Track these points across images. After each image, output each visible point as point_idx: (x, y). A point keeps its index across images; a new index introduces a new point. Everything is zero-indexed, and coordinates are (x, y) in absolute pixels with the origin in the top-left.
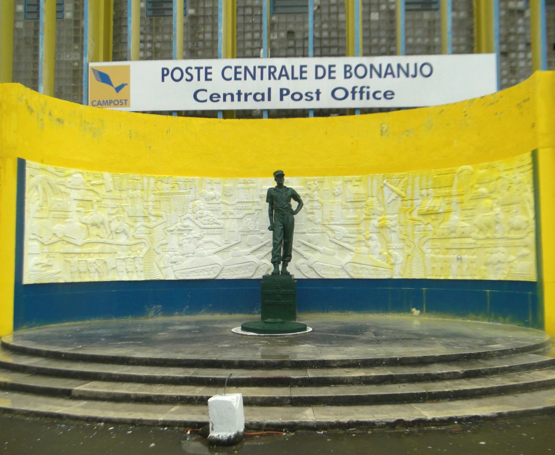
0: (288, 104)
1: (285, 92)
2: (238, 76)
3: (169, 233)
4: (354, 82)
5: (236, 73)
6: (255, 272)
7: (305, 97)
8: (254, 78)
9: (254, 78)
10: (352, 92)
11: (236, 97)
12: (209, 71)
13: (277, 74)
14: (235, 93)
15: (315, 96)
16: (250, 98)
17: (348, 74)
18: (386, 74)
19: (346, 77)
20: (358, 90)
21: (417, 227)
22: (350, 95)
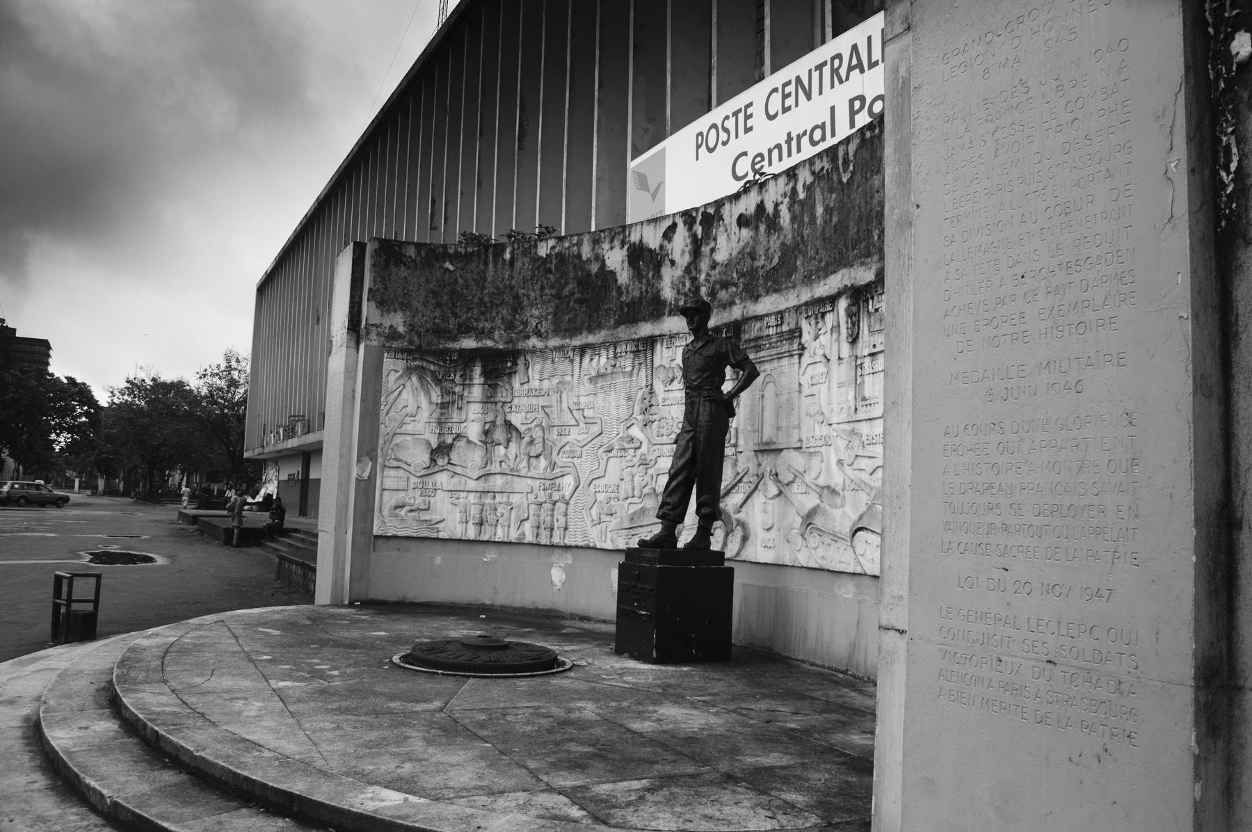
2: (790, 102)
5: (785, 96)
8: (809, 97)
9: (809, 97)
11: (785, 148)
12: (749, 111)
13: (843, 72)
14: (782, 140)
16: (805, 140)
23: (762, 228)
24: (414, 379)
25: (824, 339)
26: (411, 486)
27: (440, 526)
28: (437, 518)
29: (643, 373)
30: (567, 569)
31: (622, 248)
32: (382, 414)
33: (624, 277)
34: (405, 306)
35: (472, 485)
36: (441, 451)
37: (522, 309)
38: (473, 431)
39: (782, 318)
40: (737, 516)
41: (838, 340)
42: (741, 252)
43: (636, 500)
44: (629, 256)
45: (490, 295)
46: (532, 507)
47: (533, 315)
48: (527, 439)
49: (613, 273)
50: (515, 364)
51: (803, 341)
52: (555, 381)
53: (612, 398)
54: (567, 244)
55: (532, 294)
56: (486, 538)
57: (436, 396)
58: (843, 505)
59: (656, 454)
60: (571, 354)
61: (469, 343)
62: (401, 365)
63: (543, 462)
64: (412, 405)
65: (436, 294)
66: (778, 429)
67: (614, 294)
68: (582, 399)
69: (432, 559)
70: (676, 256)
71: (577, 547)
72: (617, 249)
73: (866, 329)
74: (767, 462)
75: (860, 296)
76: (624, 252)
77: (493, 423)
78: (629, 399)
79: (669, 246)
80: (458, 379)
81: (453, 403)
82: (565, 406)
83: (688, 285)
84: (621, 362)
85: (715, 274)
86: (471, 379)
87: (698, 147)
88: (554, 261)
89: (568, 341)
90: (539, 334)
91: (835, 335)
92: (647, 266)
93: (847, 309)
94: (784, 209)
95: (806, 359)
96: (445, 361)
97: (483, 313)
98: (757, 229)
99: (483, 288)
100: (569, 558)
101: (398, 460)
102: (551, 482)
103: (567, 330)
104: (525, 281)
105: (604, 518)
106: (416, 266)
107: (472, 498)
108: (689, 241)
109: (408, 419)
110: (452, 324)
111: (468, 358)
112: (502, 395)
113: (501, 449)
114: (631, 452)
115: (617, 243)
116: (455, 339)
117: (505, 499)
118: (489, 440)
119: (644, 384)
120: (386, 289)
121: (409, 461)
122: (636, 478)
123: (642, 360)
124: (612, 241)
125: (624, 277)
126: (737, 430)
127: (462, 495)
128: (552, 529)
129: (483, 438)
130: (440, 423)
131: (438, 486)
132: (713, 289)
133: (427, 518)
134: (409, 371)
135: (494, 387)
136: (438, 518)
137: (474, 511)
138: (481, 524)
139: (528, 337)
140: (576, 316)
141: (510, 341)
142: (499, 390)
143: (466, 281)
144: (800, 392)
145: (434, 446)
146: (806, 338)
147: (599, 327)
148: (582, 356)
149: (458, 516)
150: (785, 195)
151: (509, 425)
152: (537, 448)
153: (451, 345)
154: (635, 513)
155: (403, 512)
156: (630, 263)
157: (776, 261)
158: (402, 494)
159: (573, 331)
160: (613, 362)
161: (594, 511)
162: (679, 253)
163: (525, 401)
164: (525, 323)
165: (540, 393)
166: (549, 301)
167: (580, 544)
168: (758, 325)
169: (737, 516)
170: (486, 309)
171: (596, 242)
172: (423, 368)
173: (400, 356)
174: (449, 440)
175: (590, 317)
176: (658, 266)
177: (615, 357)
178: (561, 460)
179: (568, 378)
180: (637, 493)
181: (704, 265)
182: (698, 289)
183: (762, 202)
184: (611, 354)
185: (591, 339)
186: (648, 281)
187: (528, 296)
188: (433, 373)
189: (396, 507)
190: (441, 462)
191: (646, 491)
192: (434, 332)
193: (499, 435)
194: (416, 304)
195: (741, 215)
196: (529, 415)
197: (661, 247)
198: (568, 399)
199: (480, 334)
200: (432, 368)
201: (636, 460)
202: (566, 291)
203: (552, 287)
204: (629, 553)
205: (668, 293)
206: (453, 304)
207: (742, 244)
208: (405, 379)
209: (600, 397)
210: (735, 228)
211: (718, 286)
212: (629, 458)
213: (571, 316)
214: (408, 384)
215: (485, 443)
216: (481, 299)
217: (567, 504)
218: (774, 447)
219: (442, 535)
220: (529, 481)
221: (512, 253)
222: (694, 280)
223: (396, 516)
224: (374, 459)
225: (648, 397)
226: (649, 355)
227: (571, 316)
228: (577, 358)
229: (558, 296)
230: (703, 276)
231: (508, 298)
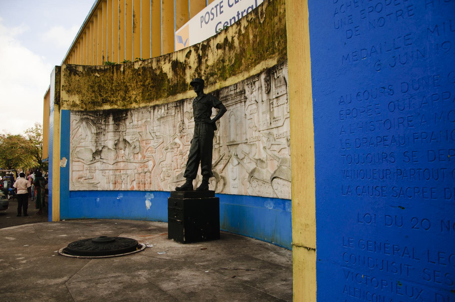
24: (84, 123)
25: (255, 93)
26: (85, 169)
27: (98, 185)
28: (96, 182)
29: (179, 115)
30: (151, 201)
31: (169, 63)
32: (71, 139)
33: (170, 75)
34: (79, 92)
35: (111, 167)
36: (97, 153)
37: (129, 91)
38: (110, 144)
39: (236, 86)
40: (221, 174)
41: (261, 93)
42: (219, 60)
43: (179, 170)
44: (172, 66)
45: (115, 86)
46: (136, 175)
47: (133, 93)
48: (133, 146)
49: (166, 74)
50: (127, 115)
51: (246, 95)
52: (144, 121)
53: (167, 127)
54: (146, 63)
55: (133, 85)
56: (117, 189)
57: (94, 129)
58: (267, 167)
60: (149, 109)
61: (107, 107)
62: (78, 117)
63: (140, 156)
64: (83, 135)
65: (92, 87)
66: (237, 135)
67: (166, 82)
68: (155, 128)
69: (96, 199)
70: (192, 64)
71: (155, 191)
72: (167, 63)
73: (274, 86)
74: (233, 150)
75: (270, 72)
76: (170, 65)
77: (119, 140)
78: (174, 126)
79: (188, 61)
80: (103, 123)
81: (101, 133)
82: (148, 131)
84: (170, 111)
85: (208, 71)
86: (108, 122)
87: (202, 22)
88: (141, 71)
89: (148, 104)
90: (136, 102)
91: (260, 91)
92: (180, 70)
93: (265, 79)
94: (236, 39)
95: (248, 103)
96: (97, 115)
97: (112, 94)
98: (225, 49)
99: (112, 83)
100: (152, 196)
101: (79, 158)
102: (144, 163)
103: (147, 99)
104: (130, 80)
105: (166, 178)
106: (83, 75)
107: (111, 172)
108: (196, 57)
109: (82, 140)
110: (100, 99)
111: (107, 113)
112: (121, 128)
113: (122, 152)
114: (176, 149)
115: (167, 61)
116: (101, 106)
117: (125, 172)
118: (117, 148)
119: (180, 120)
120: (70, 85)
121: (83, 158)
122: (178, 160)
123: (179, 110)
124: (165, 60)
125: (170, 75)
126: (219, 137)
127: (107, 171)
128: (145, 184)
129: (115, 147)
130: (96, 142)
131: (97, 168)
132: (207, 77)
133: (92, 182)
134: (82, 120)
135: (118, 125)
136: (97, 182)
137: (112, 178)
138: (116, 184)
139: (132, 103)
140: (151, 93)
141: (124, 105)
142: (121, 126)
143: (105, 81)
144: (246, 118)
145: (94, 151)
146: (247, 93)
147: (161, 97)
148: (154, 110)
149: (106, 181)
150: (236, 33)
151: (125, 141)
152: (137, 150)
153: (99, 108)
155: (82, 180)
156: (172, 69)
158: (81, 173)
159: (150, 99)
160: (167, 111)
161: (162, 176)
162: (193, 63)
163: (131, 130)
164: (130, 97)
165: (137, 127)
166: (140, 88)
167: (157, 190)
168: (227, 90)
170: (113, 92)
171: (158, 61)
172: (88, 118)
173: (77, 114)
174: (100, 149)
175: (157, 93)
176: (184, 69)
177: (168, 109)
178: (148, 154)
179: (149, 119)
180: (179, 167)
181: (203, 67)
182: (201, 77)
183: (226, 37)
184: (166, 108)
185: (158, 103)
186: (180, 76)
187: (131, 86)
188: (92, 120)
189: (79, 178)
190: (97, 158)
192: (92, 103)
193: (121, 145)
194: (84, 91)
195: (218, 44)
196: (133, 136)
197: (185, 61)
198: (149, 128)
199: (112, 103)
200: (92, 118)
201: (178, 152)
202: (147, 83)
203: (141, 81)
204: (172, 193)
206: (100, 91)
208: (80, 123)
209: (162, 127)
210: (215, 50)
211: (209, 76)
212: (175, 152)
213: (149, 93)
214: (82, 126)
215: (116, 149)
216: (111, 88)
217: (151, 173)
219: (99, 189)
220: (134, 164)
221: (124, 68)
222: (199, 74)
223: (79, 182)
224: (68, 159)
225: (182, 125)
226: (182, 107)
227: (149, 93)
228: (152, 111)
229: (143, 85)
230: (203, 72)
231: (123, 87)
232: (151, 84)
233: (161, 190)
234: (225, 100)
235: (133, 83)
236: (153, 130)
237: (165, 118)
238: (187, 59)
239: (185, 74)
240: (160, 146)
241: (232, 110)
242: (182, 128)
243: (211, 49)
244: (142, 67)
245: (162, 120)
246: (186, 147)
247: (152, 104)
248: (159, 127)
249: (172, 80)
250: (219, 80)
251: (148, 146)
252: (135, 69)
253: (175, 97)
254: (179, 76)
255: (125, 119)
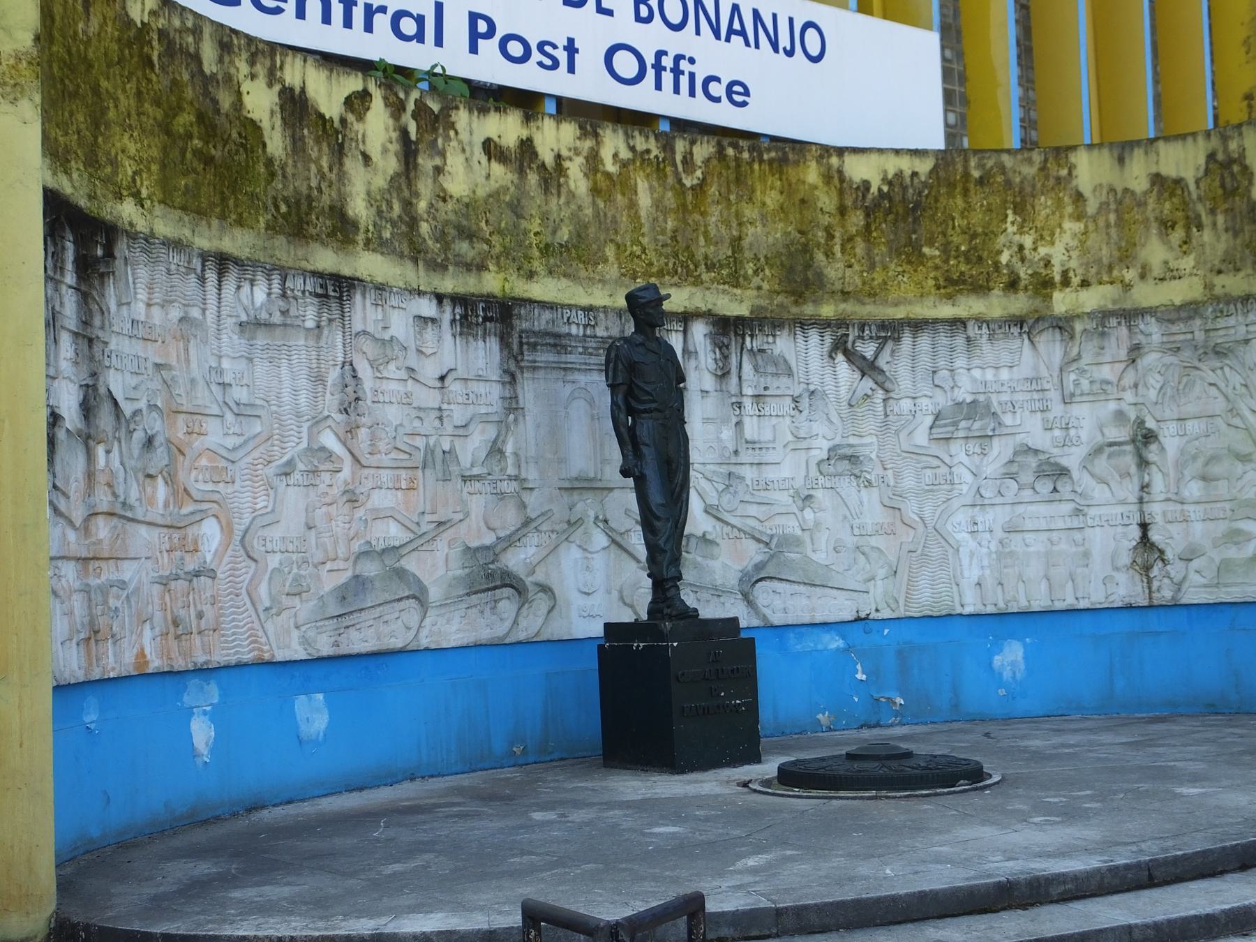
0: (489, 67)
1: (482, 27)
3: (281, 484)
4: (652, 38)
6: (516, 622)
7: (536, 56)
10: (653, 66)
15: (562, 56)
17: (644, 12)
18: (731, 31)
19: (638, 19)
20: (667, 62)
21: (929, 472)
22: (651, 73)
23: (533, 178)
30: (216, 717)
33: (276, 143)
42: (495, 195)
43: (341, 564)
44: (282, 108)
48: (139, 436)
49: (255, 126)
52: (175, 313)
59: (370, 485)
60: (197, 263)
67: (262, 169)
68: (226, 364)
71: (240, 666)
72: (261, 82)
78: (319, 379)
79: (357, 126)
83: (397, 207)
89: (187, 232)
92: (318, 141)
94: (575, 169)
100: (213, 692)
103: (184, 208)
108: (394, 135)
114: (326, 477)
123: (336, 314)
126: (516, 454)
147: (240, 223)
148: (221, 274)
152: (160, 457)
154: (345, 586)
157: (564, 234)
162: (379, 149)
166: (152, 133)
168: (547, 315)
169: (530, 579)
175: (224, 199)
176: (339, 152)
177: (284, 296)
178: (199, 486)
179: (195, 313)
180: (342, 551)
181: (425, 187)
182: (413, 222)
184: (276, 289)
186: (320, 170)
191: (356, 546)
197: (343, 121)
198: (200, 358)
201: (336, 491)
205: (359, 208)
207: (493, 185)
209: (261, 368)
211: (452, 232)
218: (599, 485)
222: (408, 205)
225: (349, 380)
228: (211, 276)
232: (197, 143)
233: (267, 656)
234: (555, 345)
235: (124, 90)
236: (221, 372)
237: (278, 331)
238: (351, 118)
239: (342, 176)
240: (256, 454)
241: (582, 384)
242: (353, 396)
243: (460, 142)
244: (162, 34)
245: (261, 340)
246: (366, 471)
247: (205, 240)
248: (243, 364)
249: (283, 168)
250: (498, 264)
251: (198, 443)
252: (130, 22)
253: (300, 253)
254: (313, 167)
255: (102, 276)
